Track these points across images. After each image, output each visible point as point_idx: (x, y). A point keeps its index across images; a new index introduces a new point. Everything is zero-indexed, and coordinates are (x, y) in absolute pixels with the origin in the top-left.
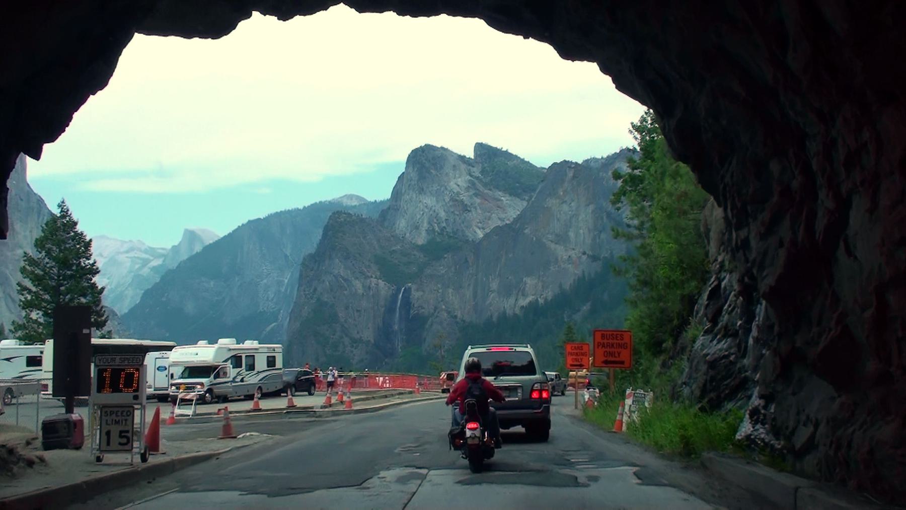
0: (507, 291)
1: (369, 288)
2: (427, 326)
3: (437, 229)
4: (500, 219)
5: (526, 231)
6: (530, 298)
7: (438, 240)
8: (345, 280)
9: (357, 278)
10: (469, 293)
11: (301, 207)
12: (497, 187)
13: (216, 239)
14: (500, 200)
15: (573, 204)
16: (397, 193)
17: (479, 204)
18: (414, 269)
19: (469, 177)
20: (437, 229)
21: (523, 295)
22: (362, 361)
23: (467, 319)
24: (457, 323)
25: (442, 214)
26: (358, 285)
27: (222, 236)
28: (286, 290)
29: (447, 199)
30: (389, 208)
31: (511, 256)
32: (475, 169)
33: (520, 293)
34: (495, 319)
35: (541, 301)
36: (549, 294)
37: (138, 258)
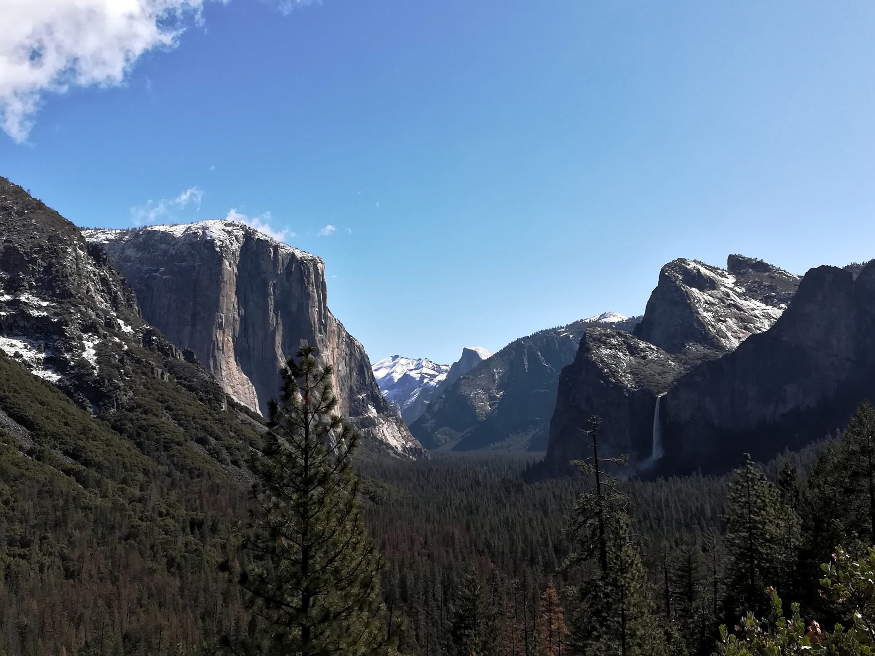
5: (784, 339)
18: (670, 378)
19: (723, 289)
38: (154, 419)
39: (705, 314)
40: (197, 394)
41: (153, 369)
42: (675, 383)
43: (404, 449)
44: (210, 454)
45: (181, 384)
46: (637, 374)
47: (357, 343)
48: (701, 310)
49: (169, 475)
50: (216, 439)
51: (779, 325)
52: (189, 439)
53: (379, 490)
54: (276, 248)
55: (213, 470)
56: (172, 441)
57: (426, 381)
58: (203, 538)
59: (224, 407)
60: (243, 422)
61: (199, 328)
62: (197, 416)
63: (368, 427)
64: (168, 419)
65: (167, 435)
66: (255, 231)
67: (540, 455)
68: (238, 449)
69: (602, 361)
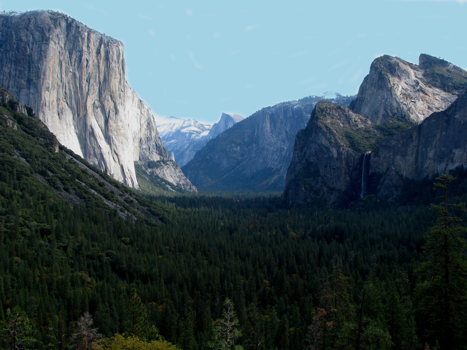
0: (440, 158)
1: (342, 153)
2: (381, 181)
3: (390, 114)
5: (457, 116)
6: (457, 165)
7: (391, 122)
9: (334, 146)
10: (411, 159)
12: (435, 86)
13: (242, 119)
16: (363, 89)
18: (373, 141)
19: (414, 78)
20: (390, 114)
21: (452, 162)
22: (334, 203)
23: (410, 177)
25: (395, 104)
26: (334, 151)
27: (245, 118)
28: (286, 154)
30: (357, 99)
31: (444, 133)
32: (420, 72)
33: (450, 161)
34: (430, 178)
37: (194, 131)
38: (9, 156)
39: (401, 96)
40: (38, 139)
41: (5, 120)
42: (377, 145)
43: (178, 184)
44: (50, 183)
45: (25, 131)
46: (351, 138)
48: (398, 93)
49: (22, 197)
50: (52, 172)
51: (453, 107)
52: (34, 172)
53: (166, 215)
54: (90, 32)
55: (52, 194)
56: (22, 172)
58: (50, 241)
59: (57, 150)
60: (70, 161)
61: (32, 91)
62: (38, 155)
63: (152, 168)
64: (18, 156)
65: (18, 168)
66: (73, 20)
67: (279, 193)
68: (68, 180)
69: (326, 127)
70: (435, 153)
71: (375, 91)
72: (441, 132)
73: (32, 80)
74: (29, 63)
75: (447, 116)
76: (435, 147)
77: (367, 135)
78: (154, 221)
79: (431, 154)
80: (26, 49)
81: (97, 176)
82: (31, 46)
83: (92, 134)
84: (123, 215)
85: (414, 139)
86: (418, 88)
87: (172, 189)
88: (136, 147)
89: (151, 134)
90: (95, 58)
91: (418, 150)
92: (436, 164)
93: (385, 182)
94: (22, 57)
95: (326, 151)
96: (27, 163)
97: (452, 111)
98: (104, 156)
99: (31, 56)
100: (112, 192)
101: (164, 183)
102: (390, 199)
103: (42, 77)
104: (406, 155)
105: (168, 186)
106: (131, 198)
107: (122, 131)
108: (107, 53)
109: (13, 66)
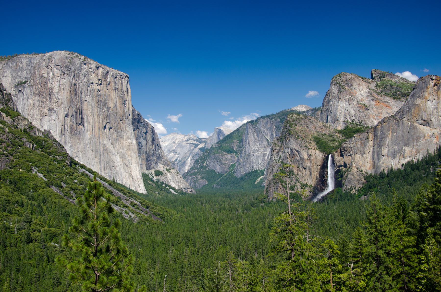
0: (393, 155)
1: (311, 155)
3: (349, 120)
4: (388, 113)
5: (404, 119)
6: (408, 159)
7: (350, 127)
8: (297, 151)
10: (368, 156)
11: (275, 113)
12: (386, 95)
14: (387, 102)
15: (434, 101)
17: (375, 105)
18: (336, 144)
19: (368, 90)
21: (403, 157)
22: (307, 197)
23: (369, 172)
24: (363, 174)
25: (353, 112)
26: (305, 155)
29: (355, 103)
32: (372, 85)
34: (386, 172)
35: (415, 161)
36: (420, 157)
39: (358, 105)
47: (150, 126)
57: (192, 148)
60: (83, 174)
61: (53, 118)
64: (36, 173)
70: (389, 150)
71: (336, 102)
72: (392, 133)
73: (53, 109)
74: (50, 94)
75: (396, 119)
76: (388, 146)
77: (331, 139)
78: (153, 220)
79: (385, 151)
80: (46, 83)
81: (106, 184)
82: (51, 81)
83: (106, 150)
84: (126, 216)
85: (370, 140)
86: (371, 98)
87: (174, 193)
88: (144, 159)
89: (155, 148)
90: (105, 88)
91: (374, 149)
92: (390, 160)
93: (349, 177)
94: (44, 90)
95: (297, 154)
96: (43, 177)
97: (401, 115)
98: (117, 168)
99: (51, 89)
100: (119, 198)
101: (168, 188)
102: (354, 190)
103: (63, 106)
104: (364, 153)
105: (171, 190)
106: (135, 202)
107: (131, 147)
108: (115, 83)
109: (36, 98)
